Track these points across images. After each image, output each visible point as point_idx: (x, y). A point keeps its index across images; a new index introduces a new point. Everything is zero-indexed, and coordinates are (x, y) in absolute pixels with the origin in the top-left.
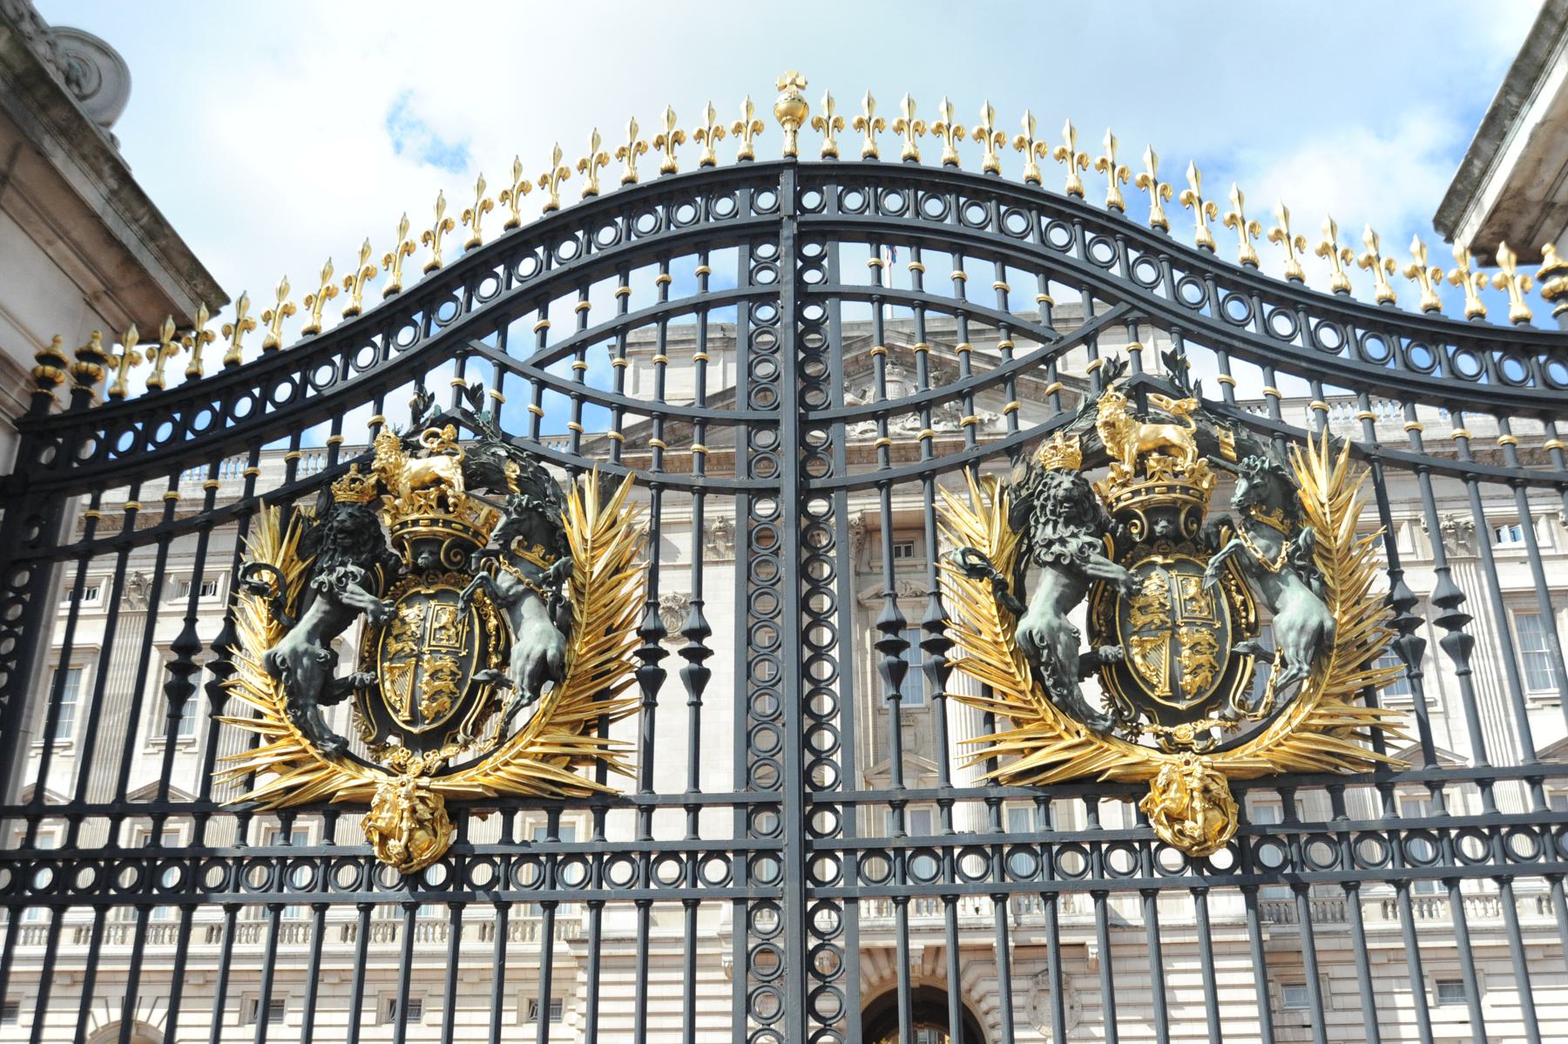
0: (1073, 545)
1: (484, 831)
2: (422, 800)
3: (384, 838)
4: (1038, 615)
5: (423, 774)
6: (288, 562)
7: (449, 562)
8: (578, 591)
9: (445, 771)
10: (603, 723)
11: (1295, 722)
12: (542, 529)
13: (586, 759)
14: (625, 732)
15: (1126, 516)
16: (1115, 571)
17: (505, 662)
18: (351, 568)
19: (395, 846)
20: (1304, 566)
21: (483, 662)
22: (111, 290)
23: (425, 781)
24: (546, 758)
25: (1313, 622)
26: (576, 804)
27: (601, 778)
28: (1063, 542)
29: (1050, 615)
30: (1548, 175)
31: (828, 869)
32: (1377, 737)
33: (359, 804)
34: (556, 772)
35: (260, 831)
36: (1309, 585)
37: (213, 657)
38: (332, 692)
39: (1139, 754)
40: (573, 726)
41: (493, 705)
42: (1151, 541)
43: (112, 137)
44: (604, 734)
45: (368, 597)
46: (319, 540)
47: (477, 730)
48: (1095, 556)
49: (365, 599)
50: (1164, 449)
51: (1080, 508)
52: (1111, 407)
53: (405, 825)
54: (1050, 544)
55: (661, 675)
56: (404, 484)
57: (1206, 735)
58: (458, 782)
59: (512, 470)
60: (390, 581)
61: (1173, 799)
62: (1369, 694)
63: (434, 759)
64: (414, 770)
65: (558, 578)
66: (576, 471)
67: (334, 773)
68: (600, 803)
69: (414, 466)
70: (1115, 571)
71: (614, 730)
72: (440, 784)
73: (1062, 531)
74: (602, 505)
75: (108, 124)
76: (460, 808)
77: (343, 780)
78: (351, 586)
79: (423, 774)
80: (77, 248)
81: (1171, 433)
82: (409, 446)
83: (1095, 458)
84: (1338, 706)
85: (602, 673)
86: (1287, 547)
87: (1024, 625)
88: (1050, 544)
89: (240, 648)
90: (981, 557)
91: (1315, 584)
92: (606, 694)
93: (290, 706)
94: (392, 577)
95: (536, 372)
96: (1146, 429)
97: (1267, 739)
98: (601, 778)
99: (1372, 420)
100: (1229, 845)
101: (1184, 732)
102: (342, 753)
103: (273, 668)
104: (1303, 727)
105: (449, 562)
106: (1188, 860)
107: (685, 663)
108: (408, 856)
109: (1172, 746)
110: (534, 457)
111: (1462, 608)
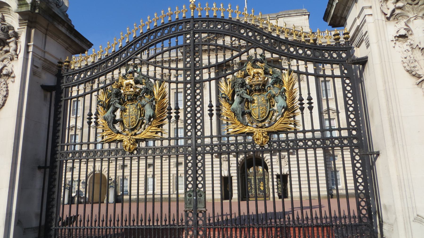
0: (241, 92)
1: (143, 145)
2: (131, 140)
3: (126, 147)
4: (235, 105)
5: (132, 135)
6: (106, 100)
7: (135, 97)
8: (156, 103)
9: (135, 134)
10: (162, 125)
11: (279, 123)
12: (149, 91)
13: (159, 132)
14: (166, 127)
15: (251, 86)
16: (248, 97)
17: (144, 116)
18: (117, 101)
19: (127, 148)
20: (282, 93)
21: (140, 116)
22: (70, 46)
23: (132, 137)
24: (152, 132)
25: (283, 105)
26: (158, 140)
27: (162, 135)
28: (239, 91)
29: (237, 105)
30: (340, 12)
31: (199, 149)
32: (295, 125)
33: (121, 141)
34: (154, 134)
35: (106, 146)
36: (283, 98)
37: (95, 116)
38: (115, 122)
39: (252, 129)
40: (156, 126)
41: (143, 123)
42: (255, 90)
43: (67, 14)
44: (162, 128)
45: (120, 106)
46: (111, 95)
47: (141, 127)
48: (245, 94)
49: (119, 106)
50: (258, 73)
51: (243, 85)
52: (249, 66)
53: (129, 144)
54: (237, 92)
55: (171, 117)
56: (124, 85)
57: (265, 125)
58: (137, 137)
59: (144, 81)
60: (122, 103)
61: (257, 136)
62: (294, 117)
63: (133, 133)
64: (130, 135)
65: (152, 101)
66: (155, 80)
67: (116, 136)
68: (162, 139)
69: (125, 82)
70: (248, 97)
71: (163, 126)
72: (134, 137)
73: (240, 89)
74: (160, 87)
75: (66, 11)
76: (138, 141)
77: (118, 137)
78: (117, 104)
79: (132, 135)
80: (62, 40)
81: (260, 71)
82: (124, 77)
83: (246, 75)
84: (287, 120)
85: (161, 117)
86: (279, 91)
87: (232, 107)
88: (237, 92)
89: (99, 115)
90: (225, 95)
91: (284, 98)
92: (162, 120)
93: (108, 125)
94: (124, 101)
95: (147, 62)
96: (255, 70)
97: (274, 126)
98: (162, 135)
99: (299, 66)
100: (267, 143)
101: (260, 125)
102: (118, 132)
103: (105, 119)
104: (280, 123)
105: (135, 97)
106: (260, 147)
107: (175, 114)
108: (130, 149)
109: (257, 127)
110: (147, 77)
111: (312, 101)
